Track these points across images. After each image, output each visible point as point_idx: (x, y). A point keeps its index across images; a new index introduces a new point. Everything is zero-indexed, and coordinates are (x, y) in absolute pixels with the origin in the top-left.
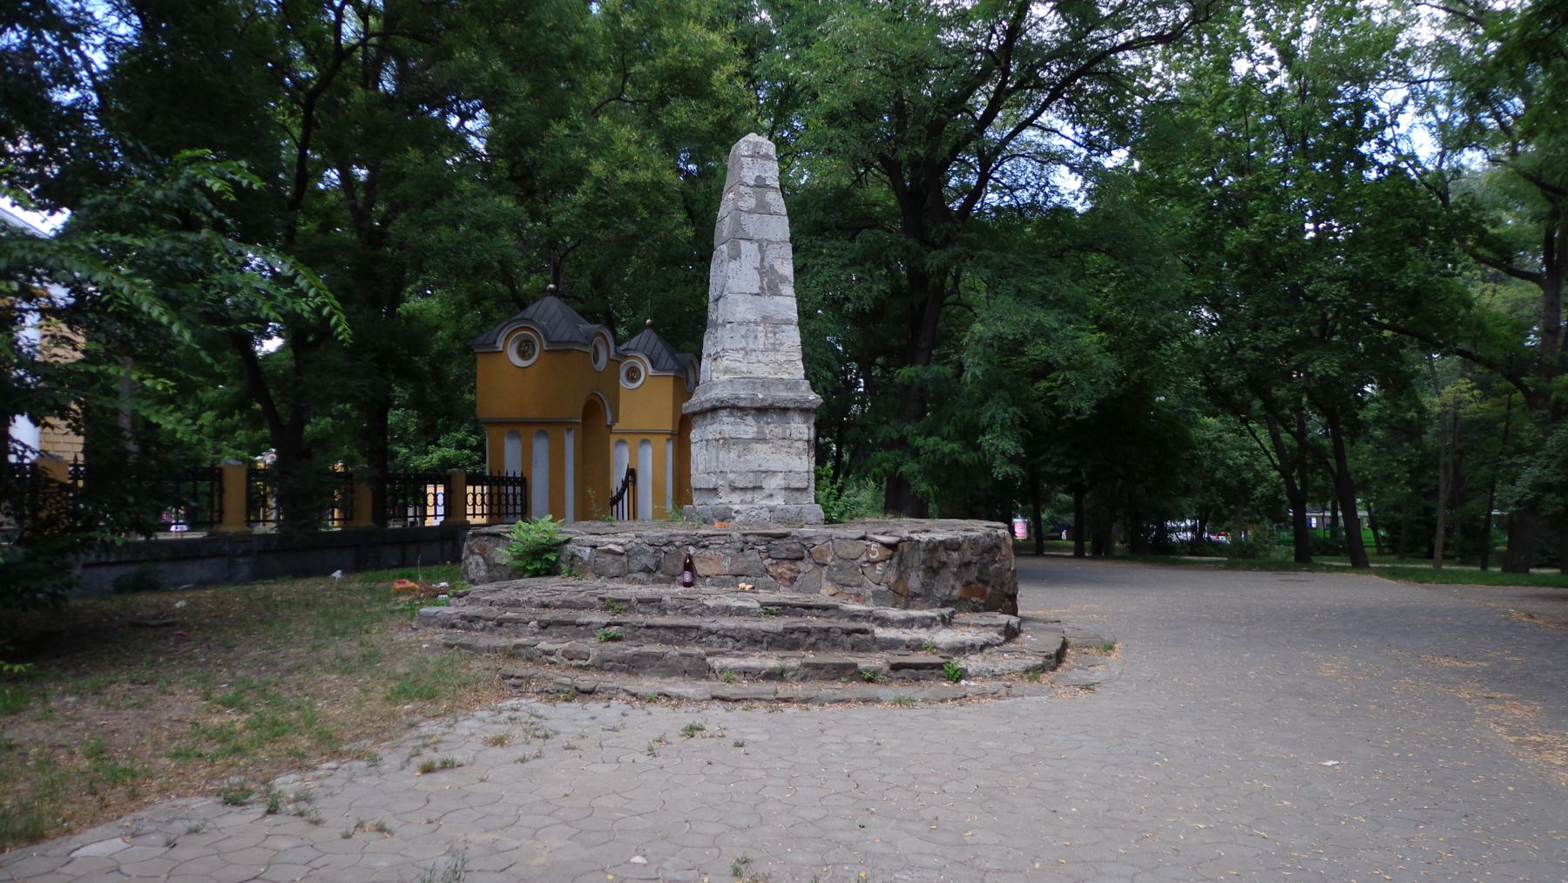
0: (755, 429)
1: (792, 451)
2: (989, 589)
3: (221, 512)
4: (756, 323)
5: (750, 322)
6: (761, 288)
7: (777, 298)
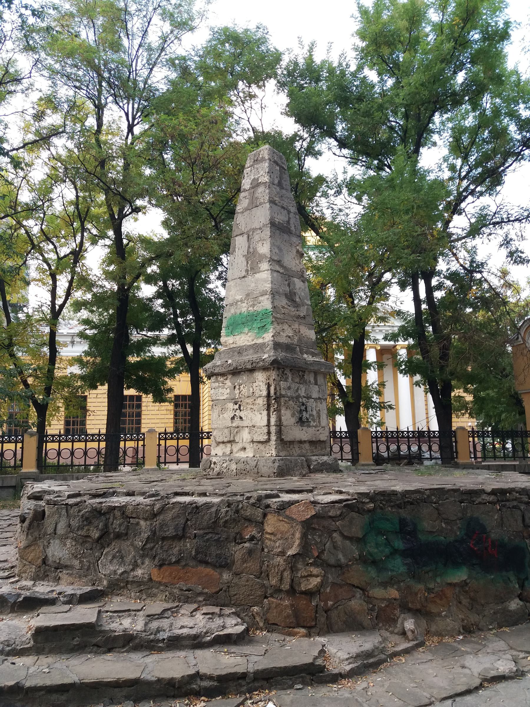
0: (228, 391)
1: (255, 407)
2: (226, 576)
3: (457, 452)
4: (242, 301)
5: (238, 301)
6: (247, 271)
7: (257, 276)
